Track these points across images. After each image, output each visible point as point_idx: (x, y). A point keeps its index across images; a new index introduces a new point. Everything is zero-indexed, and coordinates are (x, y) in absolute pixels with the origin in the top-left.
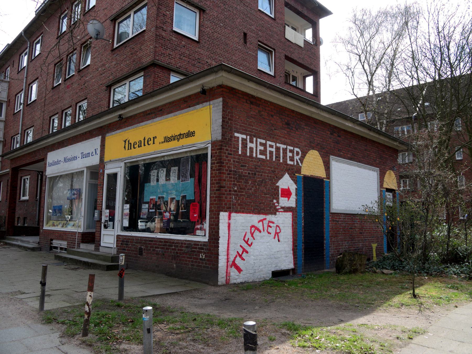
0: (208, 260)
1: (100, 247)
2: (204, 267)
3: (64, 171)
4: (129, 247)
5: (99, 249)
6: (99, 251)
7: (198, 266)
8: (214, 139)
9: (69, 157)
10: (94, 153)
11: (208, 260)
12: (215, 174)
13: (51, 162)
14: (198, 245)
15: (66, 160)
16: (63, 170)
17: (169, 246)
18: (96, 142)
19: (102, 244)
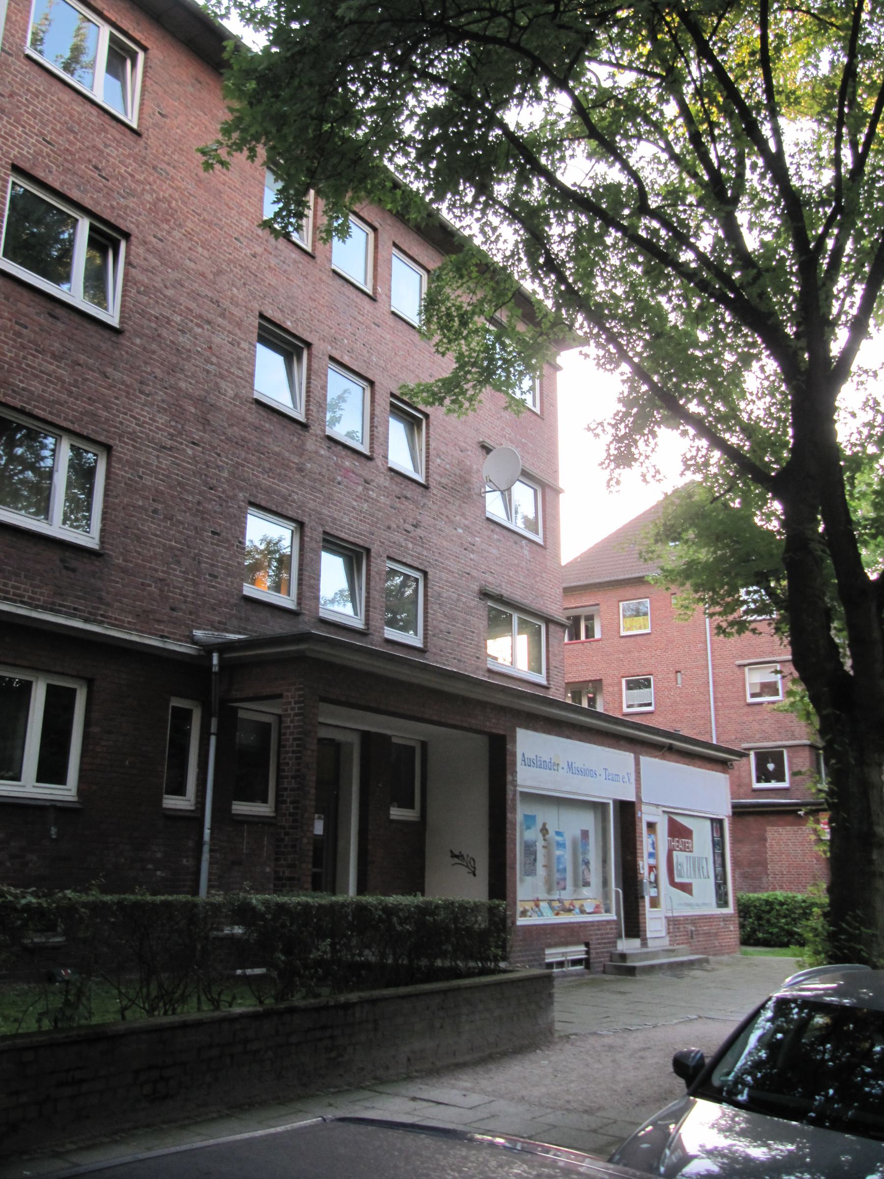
9: (578, 765)
10: (626, 779)
13: (530, 755)
16: (568, 789)
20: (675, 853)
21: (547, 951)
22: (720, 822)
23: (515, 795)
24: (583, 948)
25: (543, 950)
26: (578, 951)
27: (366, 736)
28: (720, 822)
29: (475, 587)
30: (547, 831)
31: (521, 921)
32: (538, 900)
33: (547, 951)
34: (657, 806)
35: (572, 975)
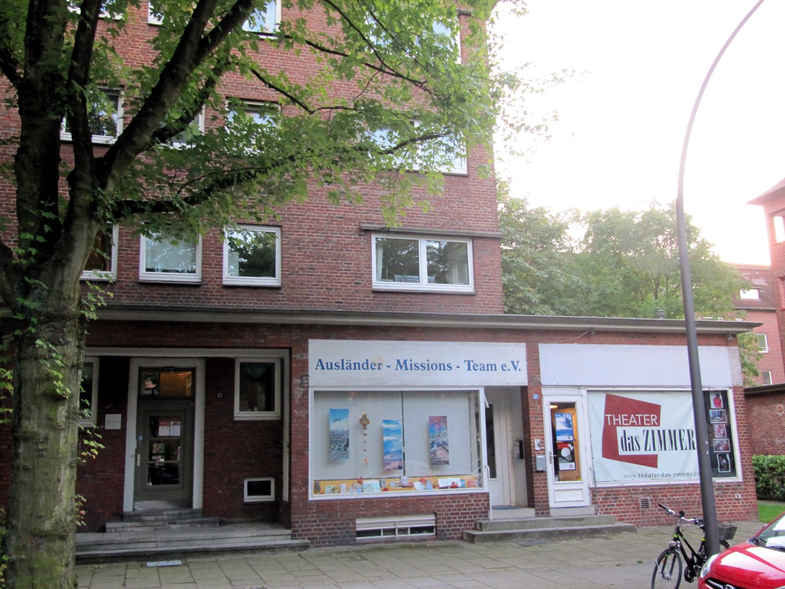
0: (744, 499)
1: (551, 510)
2: (741, 506)
3: (403, 386)
4: (620, 501)
5: (548, 513)
6: (550, 516)
7: (733, 506)
8: (735, 384)
11: (744, 499)
12: (741, 417)
14: (731, 486)
15: (402, 365)
17: (692, 491)
18: (517, 351)
19: (552, 504)
20: (620, 431)
21: (358, 521)
22: (724, 393)
23: (306, 393)
24: (433, 517)
25: (353, 521)
26: (427, 520)
27: (208, 360)
28: (724, 393)
29: (353, 226)
30: (368, 422)
31: (312, 497)
32: (361, 479)
33: (358, 521)
34: (579, 387)
35: (398, 541)
